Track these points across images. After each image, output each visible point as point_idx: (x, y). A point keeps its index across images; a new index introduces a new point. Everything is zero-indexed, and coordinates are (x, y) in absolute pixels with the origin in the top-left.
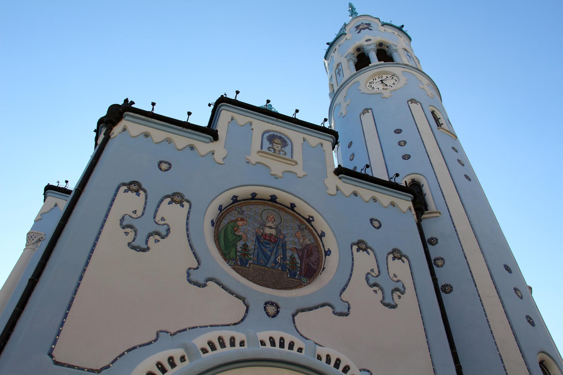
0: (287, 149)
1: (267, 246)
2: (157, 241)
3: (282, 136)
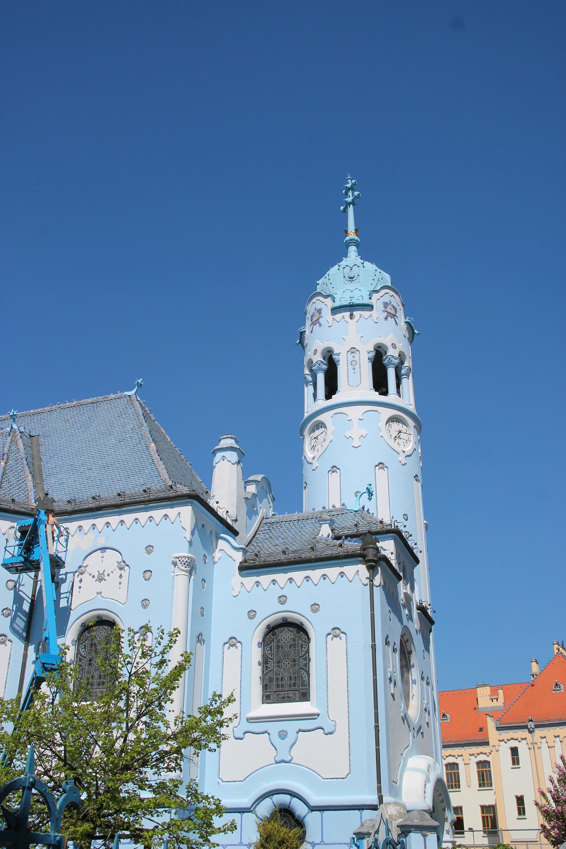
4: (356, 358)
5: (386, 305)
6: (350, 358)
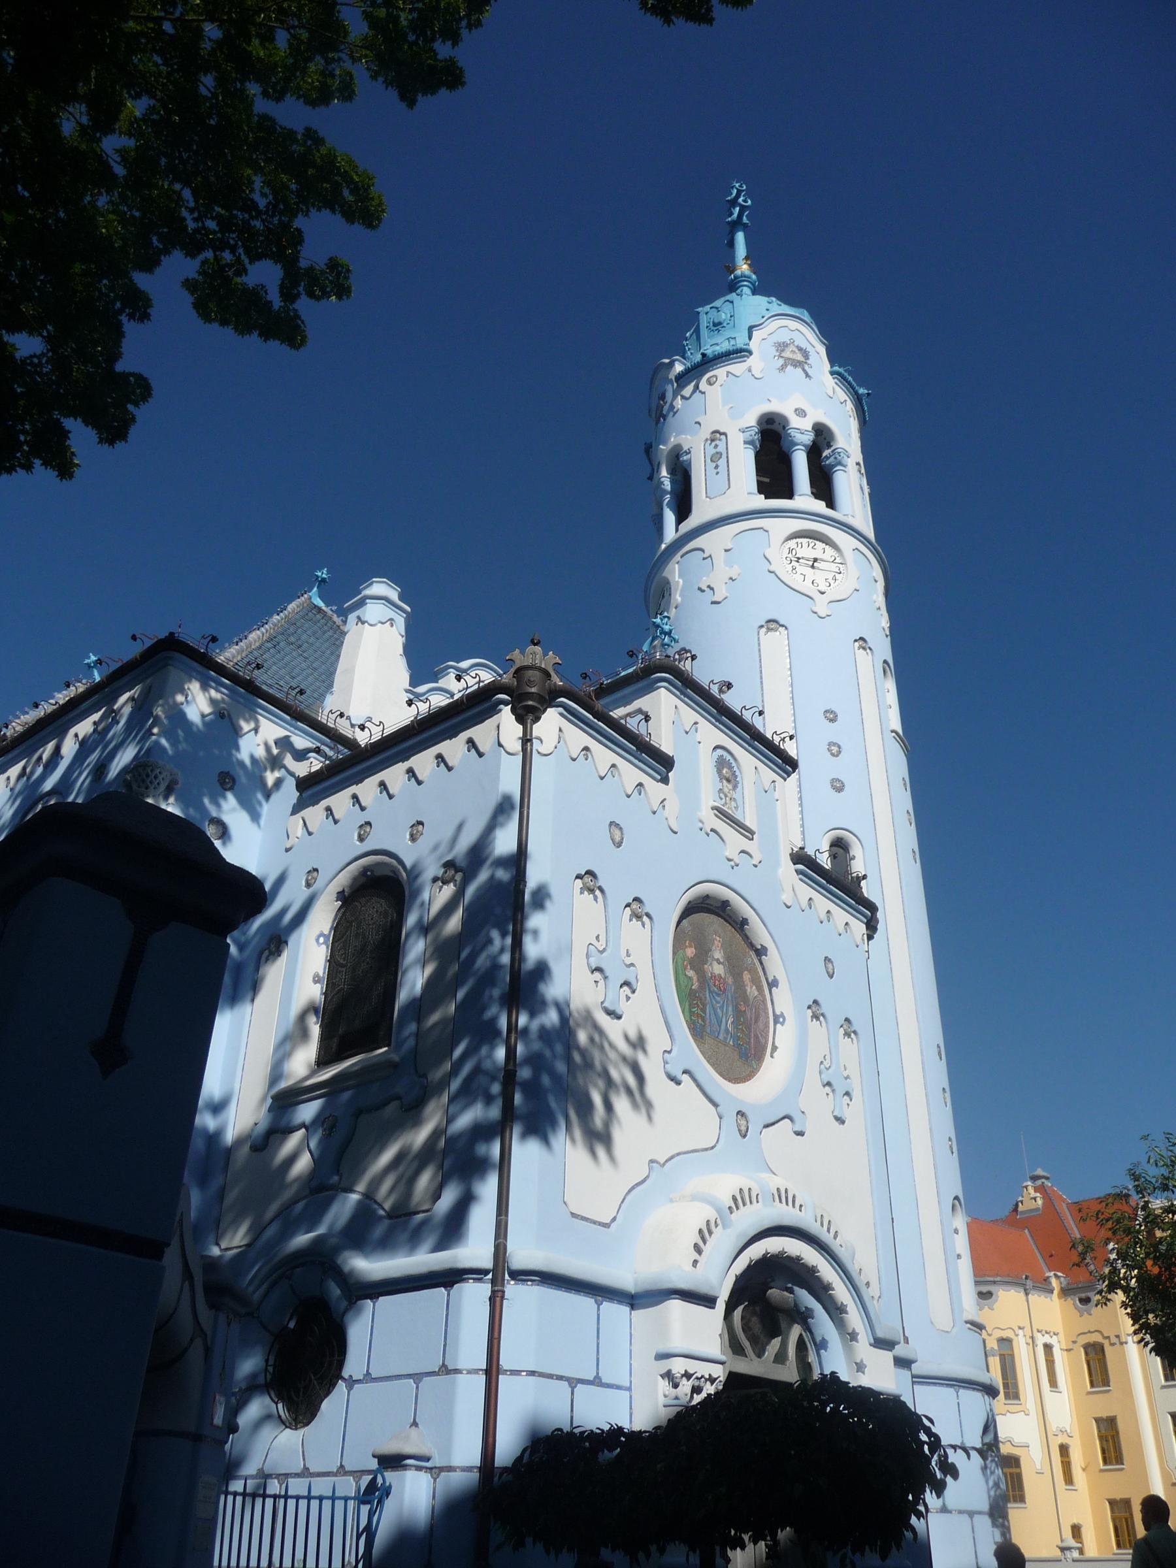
0: (737, 795)
1: (718, 999)
2: (628, 998)
3: (732, 761)
4: (721, 448)
5: (781, 347)
6: (711, 450)
